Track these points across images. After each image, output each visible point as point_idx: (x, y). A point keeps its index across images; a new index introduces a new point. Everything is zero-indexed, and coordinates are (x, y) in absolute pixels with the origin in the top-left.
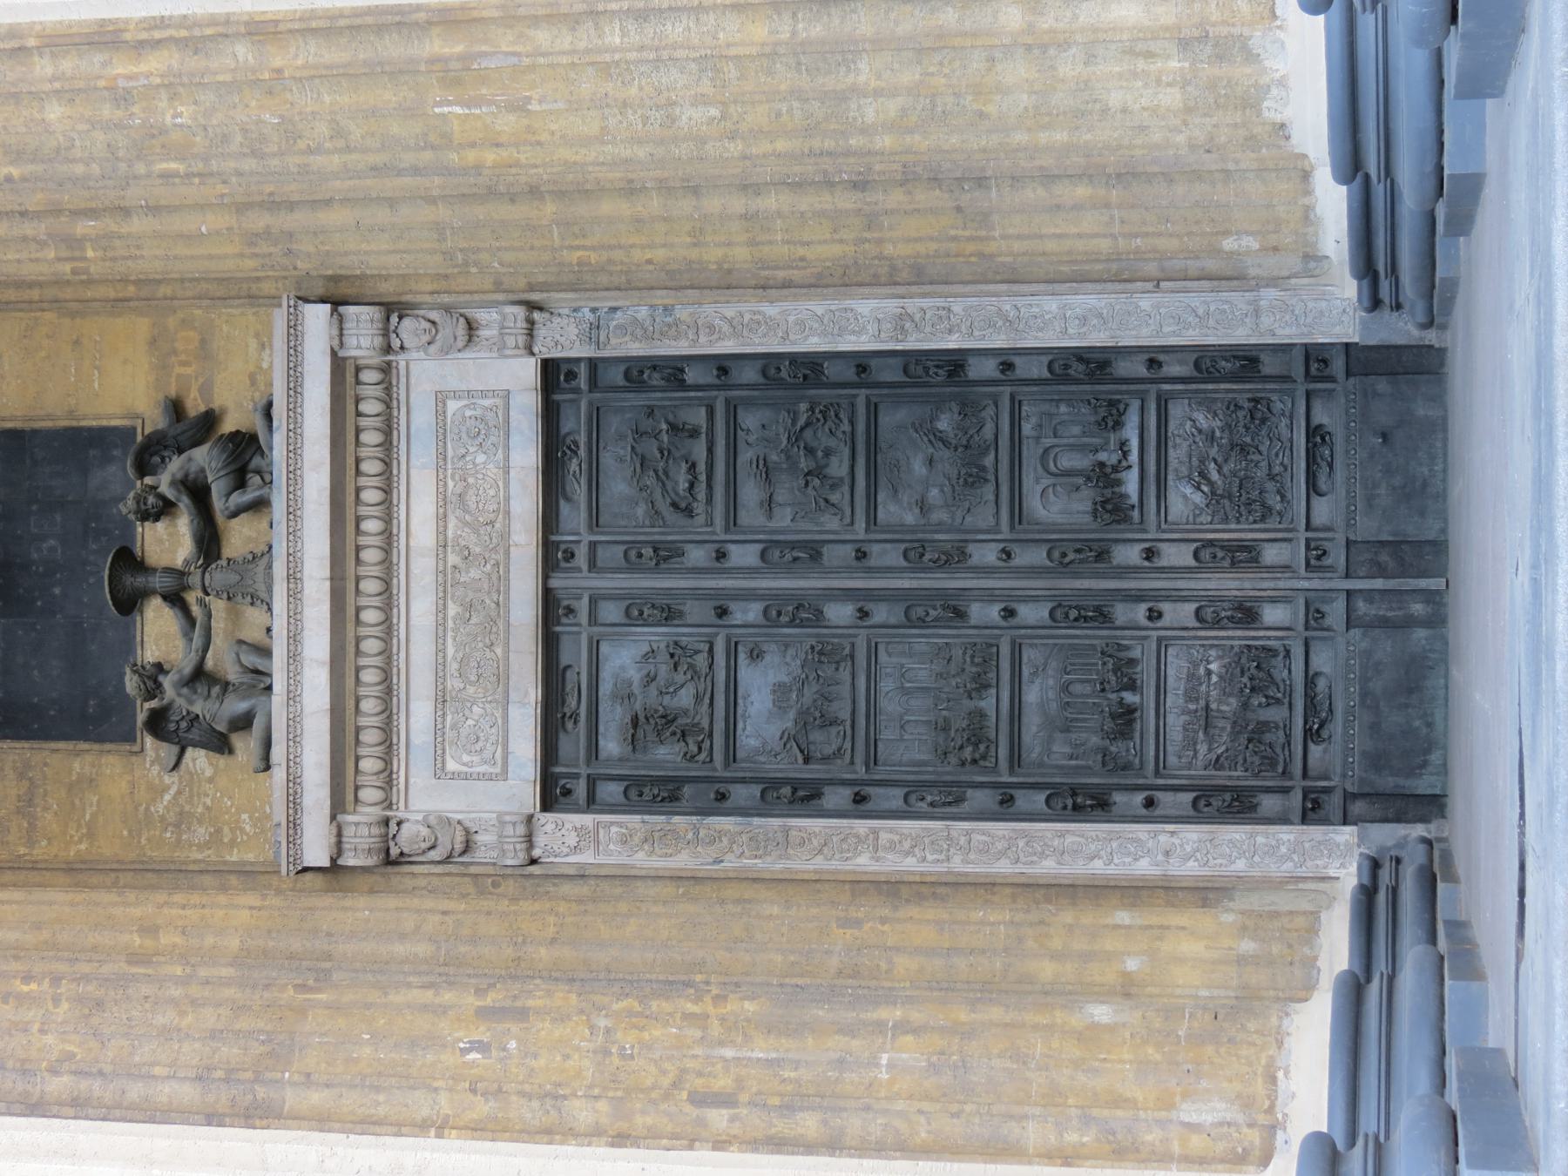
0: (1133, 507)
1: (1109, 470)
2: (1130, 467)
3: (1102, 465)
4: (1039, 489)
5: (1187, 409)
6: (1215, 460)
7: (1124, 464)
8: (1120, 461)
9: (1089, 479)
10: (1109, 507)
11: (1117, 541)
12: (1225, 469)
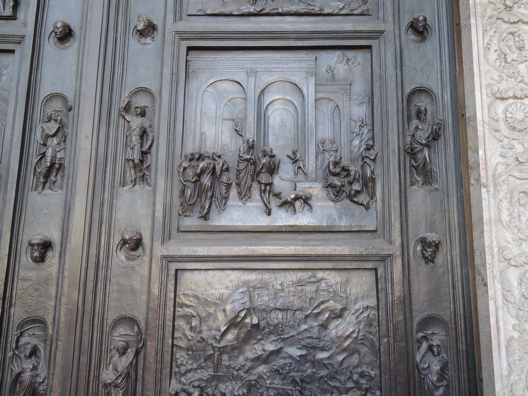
0: (205, 217)
1: (264, 178)
2: (269, 213)
3: (272, 170)
4: (241, 77)
5: (359, 305)
6: (277, 352)
7: (274, 203)
8: (278, 195)
9: (251, 147)
10: (206, 180)
11: (154, 193)
12: (262, 369)
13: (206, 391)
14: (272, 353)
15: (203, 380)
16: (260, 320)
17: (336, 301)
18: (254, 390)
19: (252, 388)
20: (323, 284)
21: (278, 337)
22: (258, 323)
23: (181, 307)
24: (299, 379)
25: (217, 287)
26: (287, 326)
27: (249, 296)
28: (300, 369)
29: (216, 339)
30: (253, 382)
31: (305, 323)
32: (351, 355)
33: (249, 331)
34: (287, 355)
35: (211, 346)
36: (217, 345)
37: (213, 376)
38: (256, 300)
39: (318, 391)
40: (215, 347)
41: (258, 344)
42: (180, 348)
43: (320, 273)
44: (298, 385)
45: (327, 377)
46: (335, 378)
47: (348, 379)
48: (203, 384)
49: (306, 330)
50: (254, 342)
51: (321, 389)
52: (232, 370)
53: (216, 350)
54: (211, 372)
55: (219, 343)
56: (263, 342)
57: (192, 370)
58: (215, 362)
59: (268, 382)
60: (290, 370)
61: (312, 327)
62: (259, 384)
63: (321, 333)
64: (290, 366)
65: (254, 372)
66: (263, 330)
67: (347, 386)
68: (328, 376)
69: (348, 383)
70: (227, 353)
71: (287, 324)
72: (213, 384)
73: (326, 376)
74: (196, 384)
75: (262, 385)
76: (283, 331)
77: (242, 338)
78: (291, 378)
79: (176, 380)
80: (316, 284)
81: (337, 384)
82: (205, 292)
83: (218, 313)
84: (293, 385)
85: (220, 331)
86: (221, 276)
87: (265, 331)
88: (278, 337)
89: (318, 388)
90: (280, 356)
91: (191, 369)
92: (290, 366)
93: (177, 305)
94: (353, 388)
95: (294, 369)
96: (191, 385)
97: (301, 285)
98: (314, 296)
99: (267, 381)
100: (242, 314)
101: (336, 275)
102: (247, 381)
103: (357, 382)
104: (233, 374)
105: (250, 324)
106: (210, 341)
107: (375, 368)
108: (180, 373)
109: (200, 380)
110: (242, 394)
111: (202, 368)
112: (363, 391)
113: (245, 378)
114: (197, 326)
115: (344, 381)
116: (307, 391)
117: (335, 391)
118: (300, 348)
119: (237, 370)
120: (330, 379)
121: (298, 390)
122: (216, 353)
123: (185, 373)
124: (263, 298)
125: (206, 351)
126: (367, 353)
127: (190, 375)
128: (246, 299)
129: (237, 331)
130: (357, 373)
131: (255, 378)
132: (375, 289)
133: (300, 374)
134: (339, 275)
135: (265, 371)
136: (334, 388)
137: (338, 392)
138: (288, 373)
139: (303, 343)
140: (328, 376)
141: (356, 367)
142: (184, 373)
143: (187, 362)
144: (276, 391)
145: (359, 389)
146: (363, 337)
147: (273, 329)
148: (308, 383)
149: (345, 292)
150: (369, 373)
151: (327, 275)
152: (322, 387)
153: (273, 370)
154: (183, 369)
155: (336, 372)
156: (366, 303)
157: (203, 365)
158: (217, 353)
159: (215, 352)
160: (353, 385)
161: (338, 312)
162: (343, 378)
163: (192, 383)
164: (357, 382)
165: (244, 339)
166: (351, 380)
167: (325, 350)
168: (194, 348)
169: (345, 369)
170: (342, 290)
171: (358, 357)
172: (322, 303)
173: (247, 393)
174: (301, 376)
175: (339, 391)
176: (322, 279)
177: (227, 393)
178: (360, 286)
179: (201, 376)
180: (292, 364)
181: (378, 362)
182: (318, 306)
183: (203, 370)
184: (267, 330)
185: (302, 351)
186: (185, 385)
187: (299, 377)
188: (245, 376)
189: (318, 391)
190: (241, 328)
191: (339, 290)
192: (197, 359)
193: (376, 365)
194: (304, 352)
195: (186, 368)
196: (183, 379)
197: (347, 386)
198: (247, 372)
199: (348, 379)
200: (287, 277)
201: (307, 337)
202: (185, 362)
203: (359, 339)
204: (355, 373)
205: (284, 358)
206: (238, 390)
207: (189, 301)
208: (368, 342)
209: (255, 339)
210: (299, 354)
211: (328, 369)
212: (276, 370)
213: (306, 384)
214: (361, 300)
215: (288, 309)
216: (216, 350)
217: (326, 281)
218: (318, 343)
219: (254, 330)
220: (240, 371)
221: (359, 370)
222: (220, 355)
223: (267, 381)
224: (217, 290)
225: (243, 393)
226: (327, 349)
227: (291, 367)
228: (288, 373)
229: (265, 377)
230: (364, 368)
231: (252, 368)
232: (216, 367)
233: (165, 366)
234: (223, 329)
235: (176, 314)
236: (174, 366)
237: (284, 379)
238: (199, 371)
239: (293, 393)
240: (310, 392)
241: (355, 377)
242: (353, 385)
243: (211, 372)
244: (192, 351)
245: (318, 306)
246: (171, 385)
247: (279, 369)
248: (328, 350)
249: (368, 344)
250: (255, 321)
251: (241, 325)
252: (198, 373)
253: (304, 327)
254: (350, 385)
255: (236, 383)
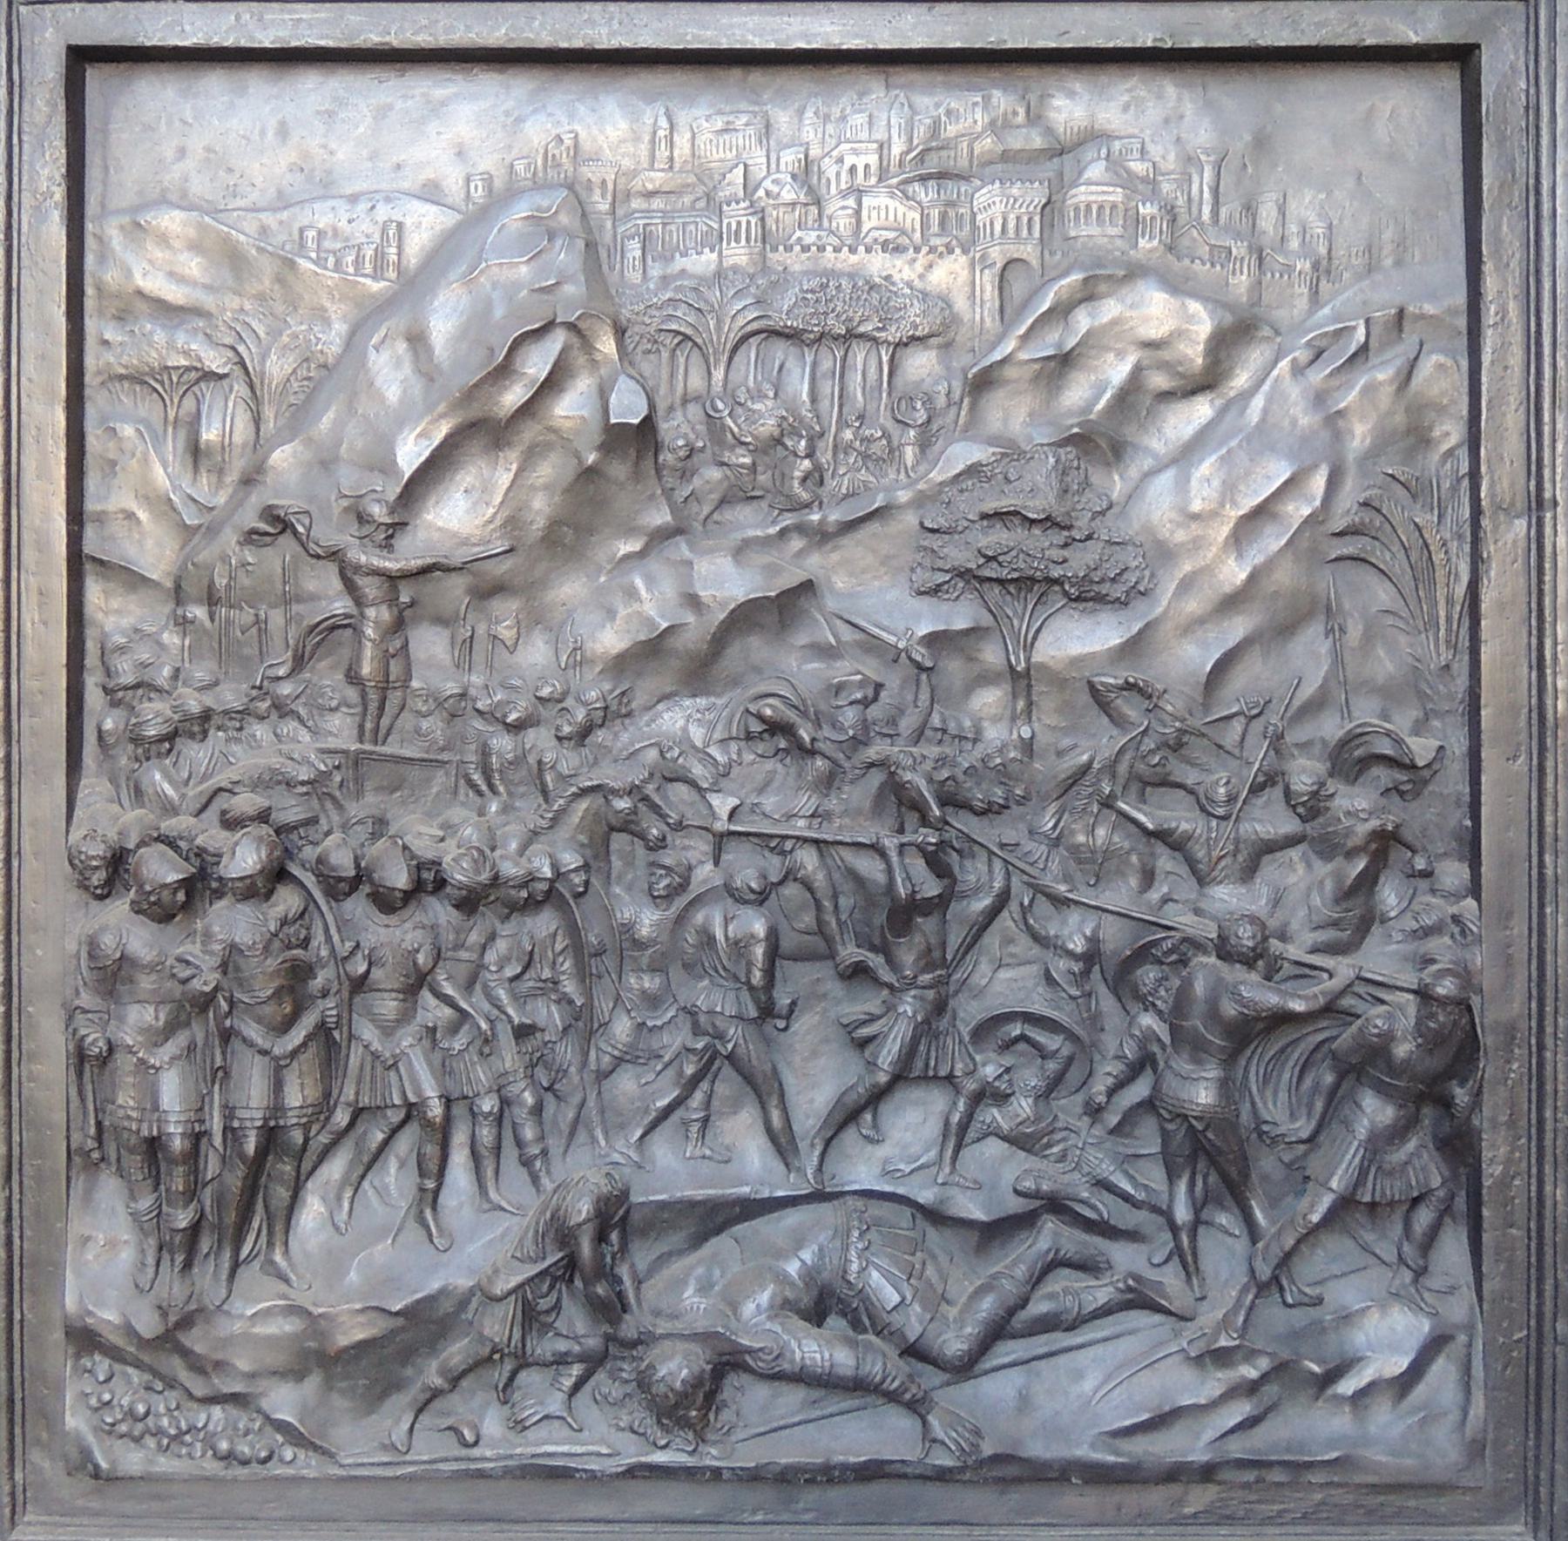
13: (310, 853)
14: (745, 617)
15: (289, 784)
16: (661, 406)
17: (1176, 286)
18: (629, 862)
19: (619, 841)
20: (1096, 171)
21: (788, 520)
22: (648, 423)
23: (121, 317)
24: (930, 780)
25: (358, 186)
26: (849, 447)
27: (581, 244)
28: (936, 720)
29: (362, 518)
30: (623, 804)
31: (969, 430)
32: (1283, 629)
33: (589, 474)
34: (848, 634)
35: (333, 569)
36: (378, 562)
37: (357, 761)
38: (635, 277)
39: (1054, 866)
40: (357, 568)
41: (654, 564)
42: (133, 580)
43: (1071, 94)
44: (925, 821)
45: (1114, 776)
46: (1165, 783)
47: (1256, 789)
48: (290, 810)
49: (973, 470)
50: (627, 547)
51: (1075, 850)
52: (478, 724)
53: (370, 588)
54: (340, 730)
55: (387, 545)
56: (680, 548)
57: (216, 720)
58: (366, 670)
59: (722, 804)
60: (865, 725)
61: (1012, 452)
62: (663, 817)
63: (1080, 492)
64: (866, 703)
65: (623, 738)
66: (685, 474)
67: (1246, 828)
68: (1123, 768)
69: (1257, 813)
70: (441, 620)
71: (848, 435)
72: (355, 810)
73: (1111, 768)
74: (246, 802)
75: (679, 827)
76: (815, 477)
77: (540, 523)
78: (876, 778)
79: (113, 780)
80: (1050, 168)
81: (1182, 818)
82: (285, 215)
83: (372, 354)
84: (891, 822)
85: (387, 466)
86: (390, 107)
87: (697, 482)
88: (788, 520)
89: (1056, 843)
90: (802, 638)
91: (206, 716)
92: (866, 703)
93: (90, 303)
94: (1292, 841)
95: (893, 722)
96: (212, 814)
97: (942, 176)
98: (1029, 251)
99: (715, 800)
100: (537, 363)
101: (1189, 108)
102: (584, 792)
103: (1312, 808)
104: (485, 752)
105: (595, 426)
106: (328, 534)
107: (1438, 714)
108: (137, 740)
109: (273, 781)
110: (547, 872)
111: (282, 709)
112: (1350, 854)
113: (563, 779)
114: (238, 438)
115: (1231, 799)
116: (981, 866)
117: (1166, 861)
118: (935, 591)
119: (517, 728)
120: (1134, 788)
121: (920, 848)
122: (371, 612)
123: (171, 737)
124: (680, 263)
125: (299, 599)
126: (1390, 620)
127: (196, 754)
128: (565, 257)
129: (504, 479)
130: (1317, 749)
131: (636, 776)
132: (1458, 200)
133: (933, 751)
134: (1209, 105)
135: (697, 734)
136: (1160, 848)
137: (1184, 870)
138: (858, 742)
139: (959, 554)
140: (1123, 768)
141: (1316, 705)
142: (161, 739)
143: (176, 674)
144: (776, 860)
145: (1327, 847)
146: (1367, 516)
147: (753, 468)
148: (988, 811)
149: (1245, 225)
150: (1398, 742)
151: (1126, 108)
152: (1081, 838)
153: (756, 727)
154: (155, 715)
155: (1176, 746)
156: (1384, 296)
157: (286, 689)
158: (378, 616)
159: (359, 602)
160: (1288, 825)
161: (1194, 354)
162: (1219, 781)
163: (221, 802)
164: (1312, 808)
165: (554, 524)
166: (1277, 792)
167: (1100, 599)
168: (221, 582)
169: (1237, 726)
170: (1224, 212)
171: (1324, 647)
172: (1088, 294)
173: (586, 867)
174: (942, 761)
175: (1191, 863)
176: (1092, 136)
177: (447, 860)
178: (1350, 183)
179: (275, 761)
180: (879, 687)
181: (1462, 682)
182: (1061, 312)
183: (289, 727)
184: (715, 474)
185: (945, 607)
186: (170, 809)
187: (928, 766)
188: (568, 760)
189: (1054, 866)
190: (531, 456)
191: (1206, 210)
192: (246, 651)
193: (1451, 697)
194: (960, 615)
195: (175, 709)
196: (157, 779)
197: (1246, 828)
198: (583, 734)
199: (1256, 789)
200: (843, 118)
201: (985, 516)
202: (166, 671)
203: (1339, 524)
204: (1304, 746)
205: (827, 652)
206: (522, 851)
207: (171, 275)
208: (1396, 548)
209: (630, 531)
210: (923, 630)
211: (1118, 721)
212: (775, 728)
213: (974, 820)
214: (1359, 277)
215: (851, 336)
216: (370, 588)
217: (1117, 145)
218: (1056, 554)
219: (619, 469)
220: (531, 736)
221: (1331, 728)
222: (399, 625)
223: (715, 800)
224: (363, 206)
225: (555, 866)
226: (1118, 591)
227: (874, 712)
228: (858, 742)
229: (698, 771)
230: (1366, 712)
231: (609, 715)
232: (373, 706)
233: (30, 684)
234: (410, 454)
235: (90, 362)
236: (93, 697)
237: (828, 782)
238: (260, 731)
239: (890, 870)
240: (998, 865)
241: (1304, 774)
242: (1288, 825)
243: (340, 730)
244: (211, 600)
245: (1061, 312)
246: (78, 813)
247: (792, 716)
248: (1123, 603)
249: (1398, 565)
250: (628, 407)
251: (530, 432)
252: (254, 744)
253: (962, 454)
254: (1269, 820)
255: (506, 809)
